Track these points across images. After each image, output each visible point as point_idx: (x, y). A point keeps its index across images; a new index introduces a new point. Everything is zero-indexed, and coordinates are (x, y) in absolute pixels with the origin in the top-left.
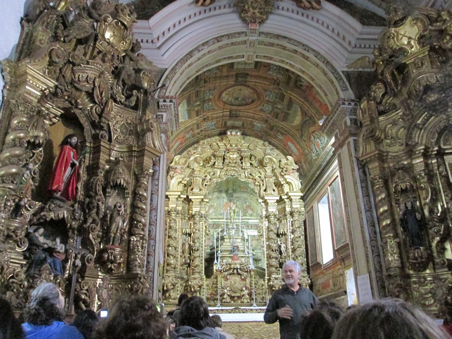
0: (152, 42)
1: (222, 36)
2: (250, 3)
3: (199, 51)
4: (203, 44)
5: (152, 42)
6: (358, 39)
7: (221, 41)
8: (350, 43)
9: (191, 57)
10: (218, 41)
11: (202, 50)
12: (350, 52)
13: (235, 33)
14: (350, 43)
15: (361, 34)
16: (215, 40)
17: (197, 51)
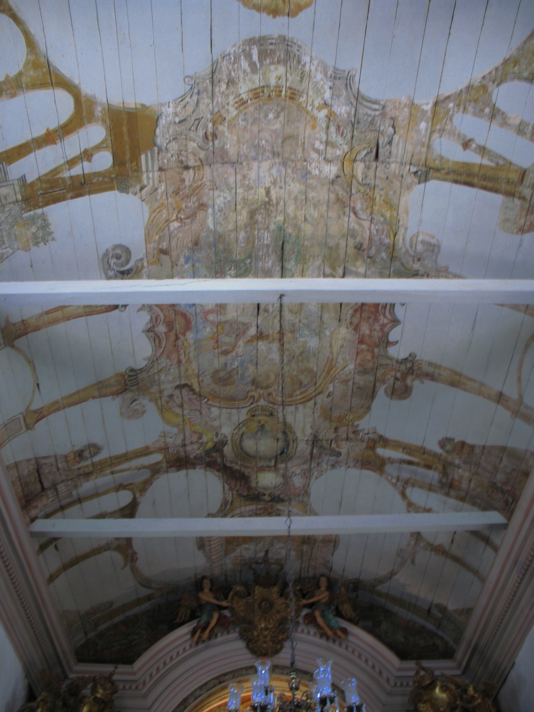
0: (137, 688)
1: (225, 674)
2: (259, 630)
3: (196, 698)
4: (201, 688)
5: (137, 688)
6: (397, 677)
7: (224, 681)
8: (388, 680)
9: (186, 707)
10: (220, 683)
11: (200, 696)
12: (389, 694)
13: (241, 669)
14: (388, 680)
15: (400, 670)
16: (217, 681)
17: (192, 699)
